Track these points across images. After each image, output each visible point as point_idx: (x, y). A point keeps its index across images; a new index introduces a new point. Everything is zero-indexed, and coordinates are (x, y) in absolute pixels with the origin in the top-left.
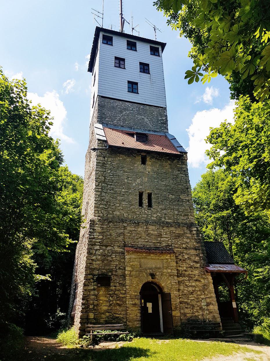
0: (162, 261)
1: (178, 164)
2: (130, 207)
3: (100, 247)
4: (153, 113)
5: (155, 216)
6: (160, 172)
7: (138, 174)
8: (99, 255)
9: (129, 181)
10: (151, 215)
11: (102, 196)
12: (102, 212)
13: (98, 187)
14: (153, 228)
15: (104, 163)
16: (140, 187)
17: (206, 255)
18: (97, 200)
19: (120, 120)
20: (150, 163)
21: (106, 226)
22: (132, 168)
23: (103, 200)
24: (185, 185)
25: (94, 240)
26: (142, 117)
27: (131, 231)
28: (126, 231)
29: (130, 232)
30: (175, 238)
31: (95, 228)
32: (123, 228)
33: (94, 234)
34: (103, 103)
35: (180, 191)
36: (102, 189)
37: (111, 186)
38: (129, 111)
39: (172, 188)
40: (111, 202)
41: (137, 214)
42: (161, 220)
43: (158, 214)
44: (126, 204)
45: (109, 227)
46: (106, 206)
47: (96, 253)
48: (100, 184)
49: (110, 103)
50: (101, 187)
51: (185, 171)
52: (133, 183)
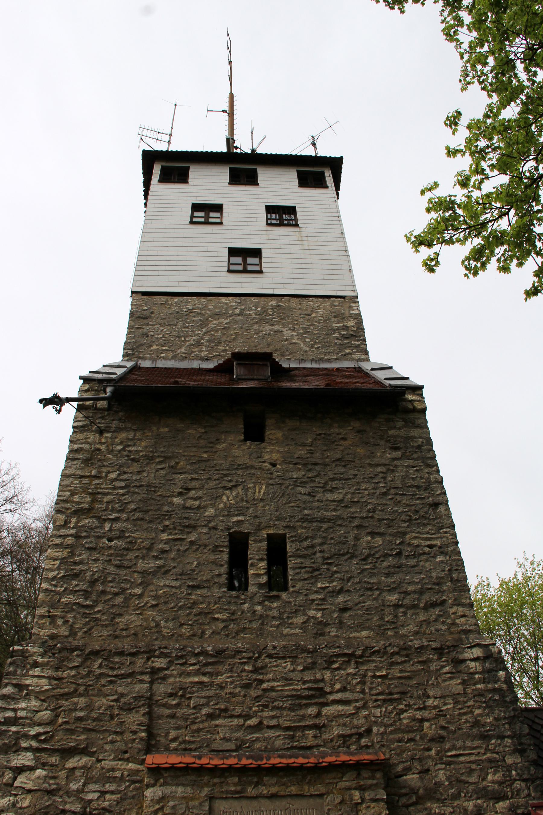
0: (319, 801)
1: (391, 428)
2: (190, 594)
3: (36, 759)
4: (313, 315)
5: (299, 620)
6: (318, 461)
7: (226, 475)
8: (29, 791)
9: (189, 503)
10: (280, 618)
11: (75, 563)
12: (67, 621)
13: (63, 532)
14: (285, 668)
15: (99, 450)
16: (235, 519)
17: (532, 755)
18: (54, 578)
19: (198, 343)
20: (280, 435)
21: (73, 673)
22: (205, 456)
23: (76, 576)
24: (424, 494)
25: (13, 729)
26: (276, 327)
27: (184, 689)
28: (161, 689)
29: (180, 693)
30: (385, 701)
31: (28, 682)
32: (147, 678)
33: (16, 706)
34: (146, 308)
35: (403, 517)
36: (77, 537)
37: (116, 526)
38: (230, 316)
39: (369, 511)
40: (111, 582)
41: (217, 619)
42: (323, 634)
43: (312, 613)
44: (174, 583)
45: (88, 675)
46: (86, 599)
47: (16, 784)
48: (74, 520)
49: (171, 305)
50: (73, 531)
51: (419, 447)
52: (205, 508)
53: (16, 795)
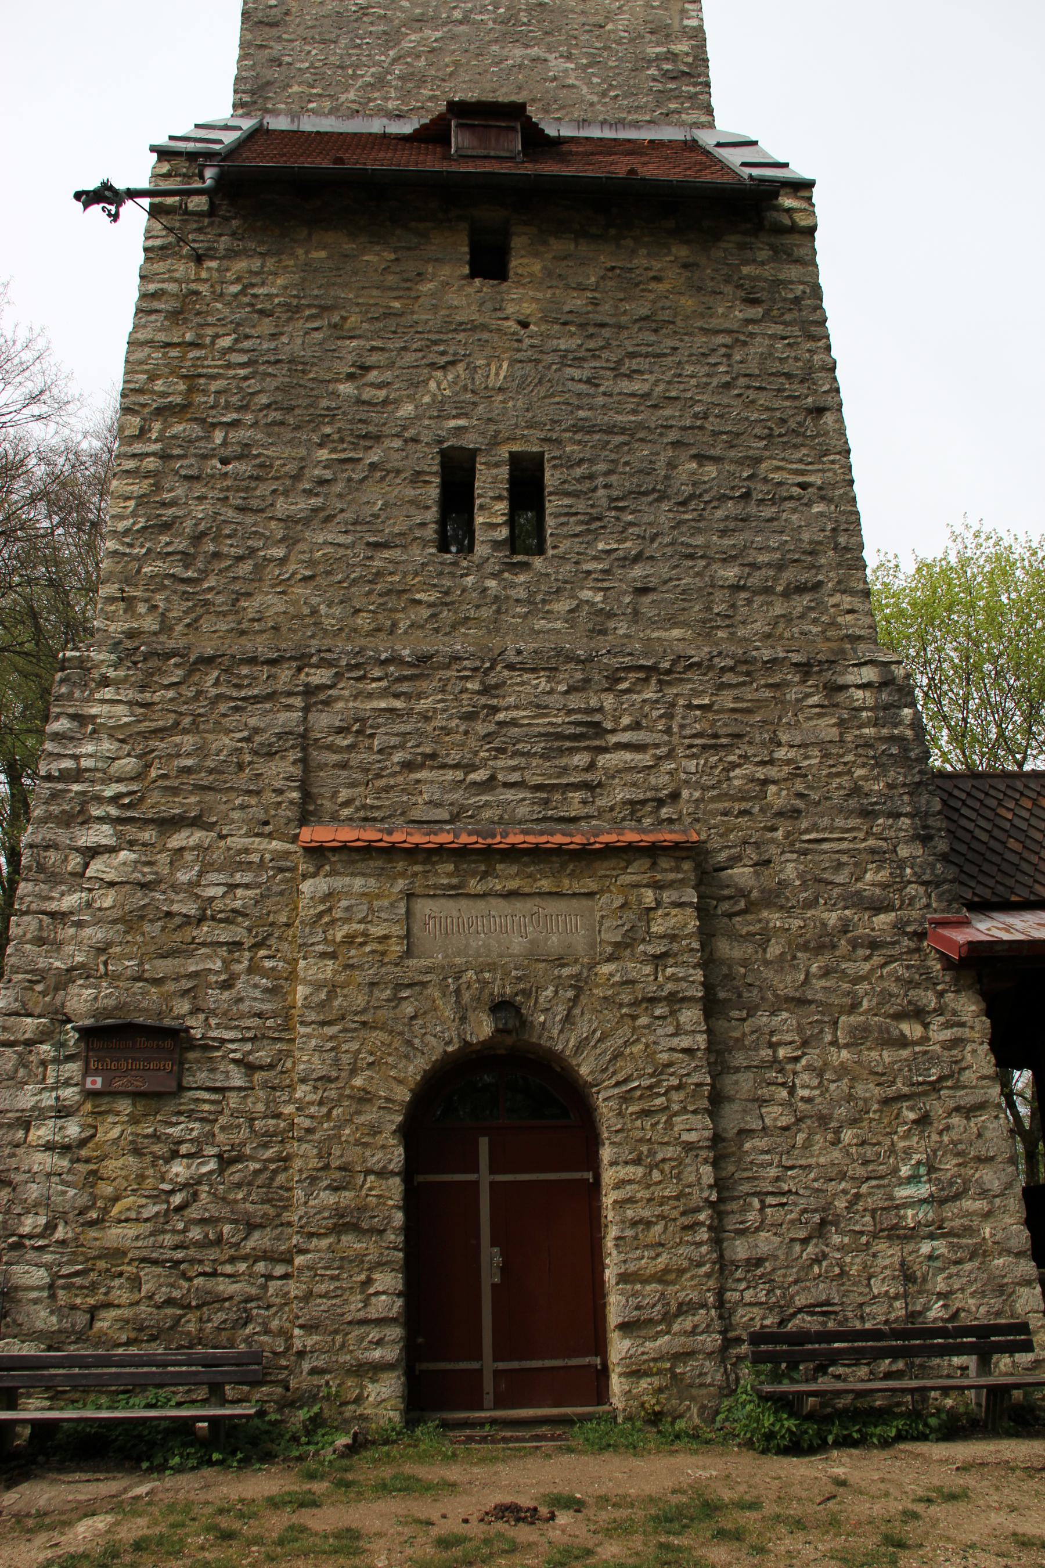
0: (586, 903)
1: (746, 263)
3: (119, 835)
4: (609, 27)
5: (562, 606)
7: (436, 343)
9: (368, 394)
10: (530, 602)
11: (164, 504)
12: (156, 607)
13: (138, 448)
14: (536, 687)
15: (196, 293)
16: (453, 423)
18: (127, 532)
19: (380, 82)
20: (537, 267)
21: (171, 694)
23: (166, 527)
24: (800, 390)
25: (76, 787)
26: (535, 51)
27: (362, 720)
28: (322, 720)
30: (704, 747)
31: (94, 711)
33: (78, 751)
35: (758, 431)
36: (164, 456)
37: (234, 435)
38: (445, 24)
39: (696, 416)
40: (229, 536)
41: (419, 602)
42: (603, 632)
43: (586, 594)
44: (342, 539)
46: (187, 567)
48: (157, 426)
50: (156, 447)
51: (797, 300)
52: (397, 402)
53: (90, 890)
